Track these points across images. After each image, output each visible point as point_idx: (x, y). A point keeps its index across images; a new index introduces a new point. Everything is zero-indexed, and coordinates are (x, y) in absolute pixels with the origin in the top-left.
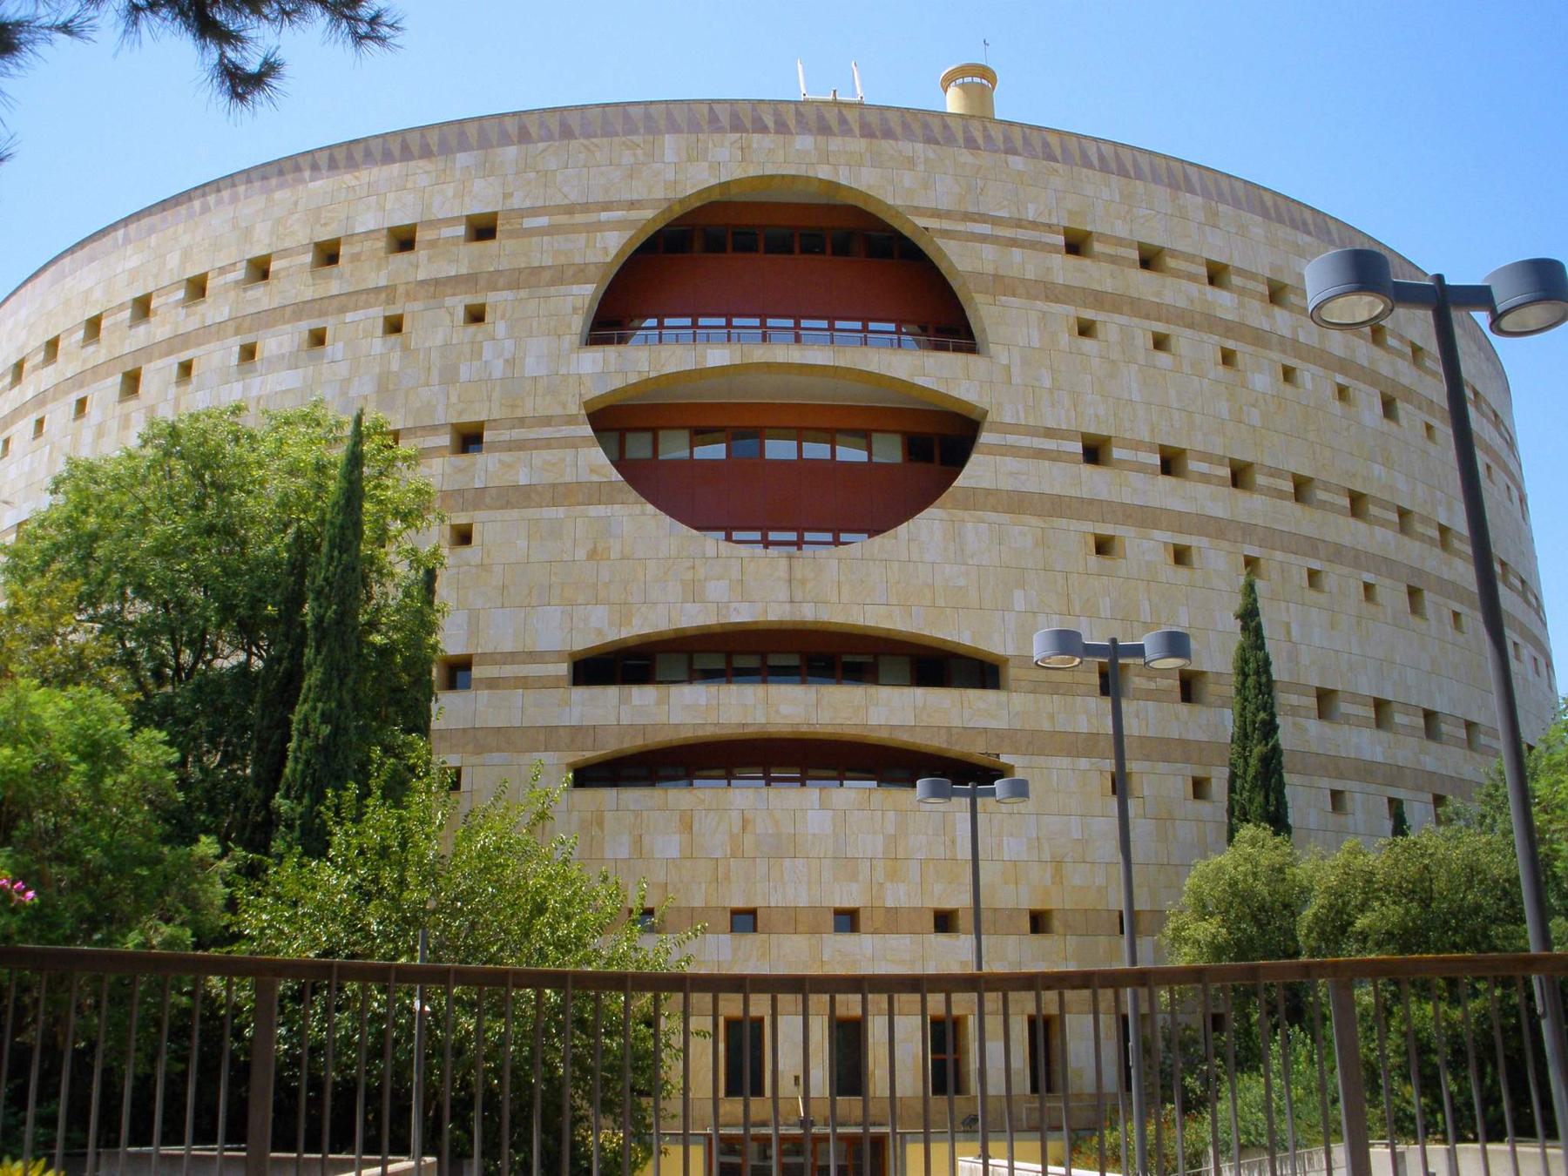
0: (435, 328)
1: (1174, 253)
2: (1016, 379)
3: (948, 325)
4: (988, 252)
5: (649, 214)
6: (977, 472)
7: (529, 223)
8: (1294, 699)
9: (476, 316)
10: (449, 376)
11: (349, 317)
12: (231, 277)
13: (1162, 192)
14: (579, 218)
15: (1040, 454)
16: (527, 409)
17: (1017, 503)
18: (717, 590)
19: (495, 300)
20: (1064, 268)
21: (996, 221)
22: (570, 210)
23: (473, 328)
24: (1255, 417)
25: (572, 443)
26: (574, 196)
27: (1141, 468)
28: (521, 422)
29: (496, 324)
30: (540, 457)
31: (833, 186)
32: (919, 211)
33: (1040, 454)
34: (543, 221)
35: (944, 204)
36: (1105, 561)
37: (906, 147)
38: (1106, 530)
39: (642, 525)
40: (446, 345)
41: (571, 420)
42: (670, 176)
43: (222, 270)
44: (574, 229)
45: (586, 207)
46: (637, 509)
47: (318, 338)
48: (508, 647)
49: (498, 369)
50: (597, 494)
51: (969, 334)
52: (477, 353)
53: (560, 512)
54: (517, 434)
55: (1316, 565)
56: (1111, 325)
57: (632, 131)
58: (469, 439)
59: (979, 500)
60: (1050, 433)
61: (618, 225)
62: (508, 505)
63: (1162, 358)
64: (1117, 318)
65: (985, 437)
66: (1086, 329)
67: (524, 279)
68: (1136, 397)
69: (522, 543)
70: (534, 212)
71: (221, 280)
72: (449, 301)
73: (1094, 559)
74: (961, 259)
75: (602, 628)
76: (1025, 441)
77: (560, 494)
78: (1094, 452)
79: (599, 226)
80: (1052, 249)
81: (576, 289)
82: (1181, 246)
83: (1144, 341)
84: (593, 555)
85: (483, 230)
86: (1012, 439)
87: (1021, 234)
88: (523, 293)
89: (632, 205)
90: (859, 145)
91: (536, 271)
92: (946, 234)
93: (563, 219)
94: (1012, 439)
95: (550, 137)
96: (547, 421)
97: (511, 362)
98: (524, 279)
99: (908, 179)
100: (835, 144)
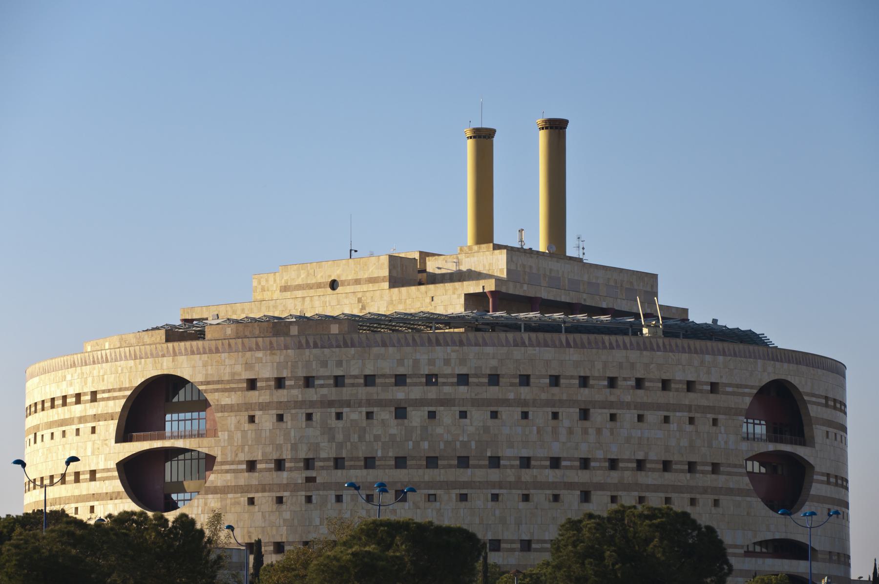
0: (704, 424)
9: (715, 422)
11: (678, 414)
12: (629, 383)
14: (740, 390)
22: (738, 386)
28: (729, 465)
43: (625, 379)
47: (666, 420)
57: (750, 357)
58: (715, 468)
70: (730, 385)
71: (625, 383)
79: (744, 395)
84: (748, 514)
85: (714, 387)
89: (752, 387)
93: (736, 389)
95: (730, 355)
97: (726, 443)
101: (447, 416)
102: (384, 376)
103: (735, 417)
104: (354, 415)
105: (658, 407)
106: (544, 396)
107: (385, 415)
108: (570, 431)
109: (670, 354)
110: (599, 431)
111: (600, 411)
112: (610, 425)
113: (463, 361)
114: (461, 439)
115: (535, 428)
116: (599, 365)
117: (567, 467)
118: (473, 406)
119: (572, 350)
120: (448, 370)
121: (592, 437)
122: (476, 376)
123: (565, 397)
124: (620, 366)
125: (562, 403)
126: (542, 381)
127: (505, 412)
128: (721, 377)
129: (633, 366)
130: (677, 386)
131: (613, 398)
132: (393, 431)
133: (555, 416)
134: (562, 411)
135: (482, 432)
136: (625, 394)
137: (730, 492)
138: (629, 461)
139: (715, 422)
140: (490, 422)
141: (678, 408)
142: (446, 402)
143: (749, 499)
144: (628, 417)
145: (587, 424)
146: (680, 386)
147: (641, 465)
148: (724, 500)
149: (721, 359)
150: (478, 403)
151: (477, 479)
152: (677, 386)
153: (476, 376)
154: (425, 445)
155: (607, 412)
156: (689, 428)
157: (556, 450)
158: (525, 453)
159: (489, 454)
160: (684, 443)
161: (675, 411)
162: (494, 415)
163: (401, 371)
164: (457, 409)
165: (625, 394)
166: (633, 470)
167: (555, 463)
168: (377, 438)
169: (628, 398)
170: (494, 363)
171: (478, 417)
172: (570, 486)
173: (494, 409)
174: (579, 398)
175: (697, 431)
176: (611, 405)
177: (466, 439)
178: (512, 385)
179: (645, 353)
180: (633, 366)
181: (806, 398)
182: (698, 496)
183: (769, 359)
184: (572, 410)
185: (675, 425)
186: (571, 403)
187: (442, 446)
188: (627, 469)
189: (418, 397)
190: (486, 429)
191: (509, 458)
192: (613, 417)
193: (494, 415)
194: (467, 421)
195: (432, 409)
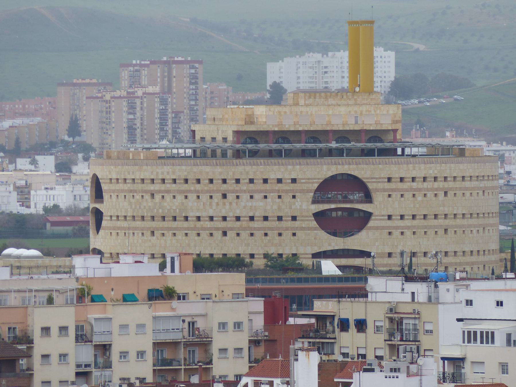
0: (287, 198)
1: (406, 178)
2: (378, 207)
3: (368, 198)
4: (375, 184)
5: (322, 181)
6: (371, 224)
7: (302, 181)
8: (420, 255)
9: (294, 197)
10: (290, 208)
11: (271, 194)
12: (245, 181)
13: (405, 166)
14: (310, 181)
15: (381, 219)
16: (304, 214)
17: (377, 228)
18: (333, 244)
19: (297, 195)
20: (387, 186)
21: (376, 178)
22: (309, 179)
23: (293, 199)
24: (417, 206)
25: (311, 220)
26: (309, 177)
27: (397, 219)
28: (303, 216)
29: (298, 199)
32: (364, 178)
33: (381, 219)
34: (304, 181)
35: (368, 176)
36: (390, 236)
37: (362, 166)
38: (390, 231)
39: (322, 234)
41: (311, 217)
43: (244, 179)
44: (309, 183)
45: (311, 179)
47: (266, 197)
48: (303, 252)
49: (298, 207)
50: (315, 229)
51: (371, 198)
52: (295, 204)
53: (309, 232)
54: (302, 218)
55: (426, 230)
56: (394, 194)
57: (318, 165)
58: (294, 218)
59: (371, 228)
60: (383, 216)
62: (301, 230)
63: (402, 199)
64: (395, 193)
65: (373, 218)
66: (390, 196)
67: (302, 191)
68: (397, 207)
69: (304, 236)
71: (243, 181)
72: (289, 194)
73: (388, 236)
74: (370, 186)
75: (316, 250)
76: (379, 218)
78: (390, 217)
80: (385, 182)
81: (310, 194)
82: (408, 176)
83: (399, 196)
84: (315, 239)
85: (294, 181)
86: (377, 218)
87: (380, 180)
89: (319, 179)
90: (355, 166)
91: (304, 190)
92: (369, 182)
93: (307, 181)
94: (377, 218)
95: (304, 165)
96: (307, 217)
97: (301, 206)
98: (302, 191)
99: (363, 172)
100: (351, 166)
101: (168, 197)
105: (261, 191)
106: (206, 188)
108: (217, 204)
110: (231, 204)
111: (231, 194)
113: (174, 173)
115: (202, 203)
116: (231, 173)
117: (216, 221)
121: (227, 206)
123: (215, 189)
124: (241, 173)
128: (298, 175)
129: (247, 173)
130: (271, 181)
132: (150, 204)
133: (211, 197)
136: (244, 186)
137: (303, 229)
138: (245, 217)
139: (294, 197)
140: (184, 201)
142: (168, 191)
143: (316, 232)
144: (245, 197)
145: (225, 200)
146: (273, 181)
147: (252, 218)
148: (298, 233)
149: (298, 167)
152: (271, 181)
154: (160, 211)
155: (234, 195)
156: (278, 200)
159: (184, 215)
160: (275, 207)
162: (186, 197)
164: (172, 195)
165: (244, 186)
166: (247, 221)
167: (211, 218)
168: (145, 207)
169: (245, 188)
170: (186, 173)
171: (180, 198)
172: (217, 229)
173: (186, 194)
174: (222, 189)
175: (282, 202)
176: (237, 191)
178: (193, 183)
179: (254, 167)
180: (247, 173)
181: (364, 180)
182: (282, 232)
183: (333, 165)
184: (218, 194)
186: (218, 191)
187: (166, 211)
188: (244, 221)
190: (183, 204)
191: (192, 217)
193: (186, 197)
195: (163, 194)
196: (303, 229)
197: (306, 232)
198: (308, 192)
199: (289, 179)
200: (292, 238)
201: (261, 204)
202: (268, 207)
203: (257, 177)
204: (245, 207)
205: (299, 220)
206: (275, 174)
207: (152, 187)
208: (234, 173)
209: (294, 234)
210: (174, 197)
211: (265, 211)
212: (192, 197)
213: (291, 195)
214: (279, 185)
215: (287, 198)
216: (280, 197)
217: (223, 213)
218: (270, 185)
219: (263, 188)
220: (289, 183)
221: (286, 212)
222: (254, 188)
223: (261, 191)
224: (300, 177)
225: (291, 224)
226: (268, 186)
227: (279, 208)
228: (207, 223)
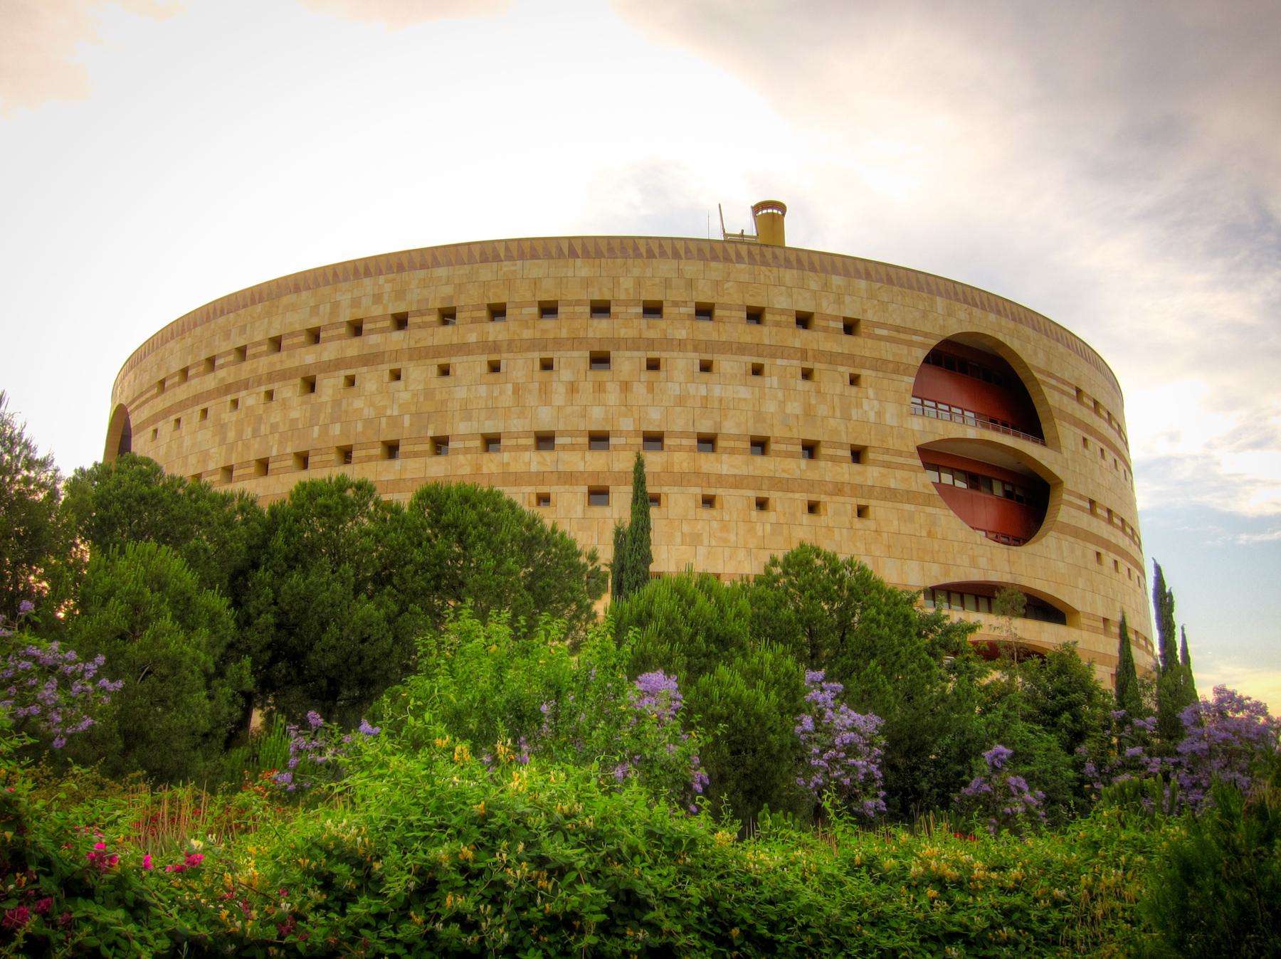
0: (832, 382)
4: (1056, 395)
9: (854, 380)
10: (847, 417)
11: (779, 362)
12: (683, 310)
14: (902, 336)
16: (891, 443)
22: (898, 329)
26: (898, 322)
28: (887, 451)
30: (900, 474)
31: (1002, 345)
34: (884, 332)
40: (842, 395)
42: (941, 322)
43: (676, 304)
46: (946, 512)
47: (757, 371)
49: (872, 416)
52: (859, 405)
54: (887, 458)
58: (858, 455)
61: (922, 345)
62: (885, 499)
71: (675, 310)
72: (841, 369)
77: (911, 497)
79: (910, 344)
81: (906, 379)
84: (930, 535)
85: (850, 327)
88: (880, 374)
89: (926, 335)
90: (1011, 324)
91: (885, 361)
93: (894, 334)
95: (881, 281)
96: (900, 453)
98: (880, 365)
100: (1004, 321)
101: (372, 380)
102: (292, 334)
103: (895, 376)
104: (250, 399)
105: (741, 349)
106: (527, 334)
107: (289, 391)
108: (573, 388)
109: (763, 268)
110: (626, 387)
111: (628, 354)
112: (647, 375)
113: (400, 294)
114: (389, 412)
115: (510, 386)
116: (627, 283)
117: (564, 447)
118: (411, 359)
119: (579, 262)
120: (377, 311)
121: (613, 396)
122: (420, 313)
123: (564, 333)
124: (667, 283)
125: (558, 343)
126: (525, 311)
127: (459, 365)
128: (864, 311)
129: (690, 284)
130: (777, 318)
131: (811, 475)
132: (295, 414)
133: (547, 365)
134: (560, 357)
135: (421, 399)
136: (676, 325)
137: (890, 495)
138: (684, 434)
139: (854, 380)
140: (437, 382)
141: (779, 351)
142: (370, 359)
143: (930, 510)
144: (681, 365)
145: (602, 375)
146: (784, 318)
147: (708, 442)
148: (878, 509)
149: (862, 284)
150: (418, 354)
151: (408, 475)
152: (777, 318)
153: (420, 313)
154: (336, 429)
155: (642, 356)
156: (802, 385)
157: (545, 419)
158: (490, 427)
159: (431, 433)
160: (794, 408)
161: (774, 356)
162: (445, 371)
163: (314, 323)
164: (385, 369)
165: (676, 325)
166: (691, 450)
167: (545, 440)
168: (274, 427)
169: (682, 334)
170: (448, 290)
171: (419, 375)
172: (569, 478)
173: (443, 361)
174: (591, 334)
175: (818, 392)
176: (651, 344)
177: (396, 413)
178: (475, 321)
179: (713, 264)
180: (690, 284)
181: (1036, 375)
182: (823, 498)
183: (958, 300)
184: (576, 354)
185: (775, 379)
186: (575, 342)
187: (360, 428)
188: (679, 448)
189: (333, 358)
190: (429, 394)
191: (464, 437)
192: (653, 365)
193: (445, 371)
194: (400, 384)
195: (350, 372)
196: (890, 495)
197: (900, 505)
198: (896, 371)
199: (835, 318)
200: (858, 523)
201: (744, 392)
202: (771, 407)
203: (726, 300)
204: (681, 401)
205: (875, 463)
206: (790, 296)
207: (309, 357)
208: (639, 283)
209: (862, 512)
210: (396, 375)
211: (759, 416)
212: (470, 368)
213: (846, 371)
214: (804, 333)
215: (832, 382)
216: (807, 375)
217: (597, 419)
218: (774, 330)
219: (746, 338)
220: (836, 331)
221: (834, 430)
222: (715, 336)
223: (741, 349)
224: (870, 316)
225: (847, 472)
226: (764, 334)
227: (809, 413)
228: (526, 456)
